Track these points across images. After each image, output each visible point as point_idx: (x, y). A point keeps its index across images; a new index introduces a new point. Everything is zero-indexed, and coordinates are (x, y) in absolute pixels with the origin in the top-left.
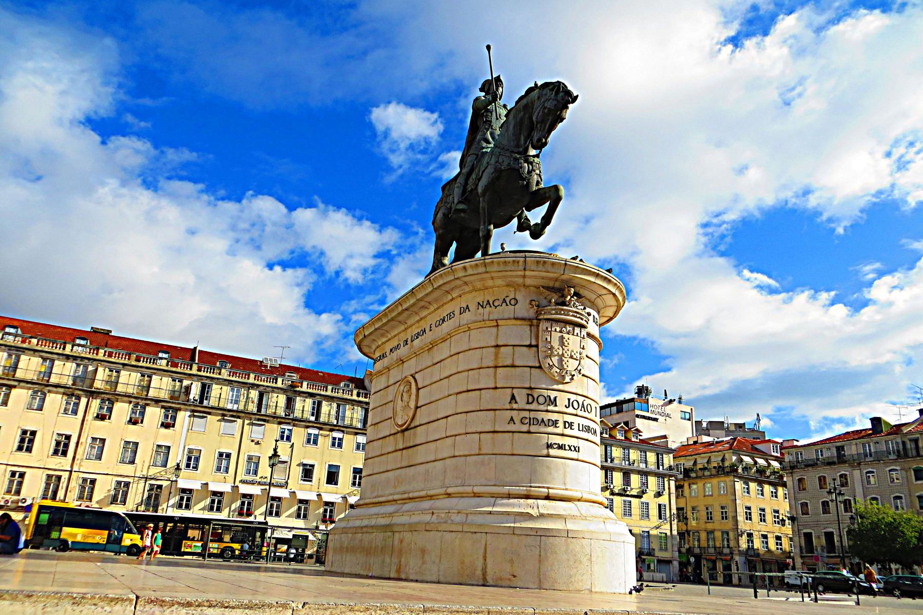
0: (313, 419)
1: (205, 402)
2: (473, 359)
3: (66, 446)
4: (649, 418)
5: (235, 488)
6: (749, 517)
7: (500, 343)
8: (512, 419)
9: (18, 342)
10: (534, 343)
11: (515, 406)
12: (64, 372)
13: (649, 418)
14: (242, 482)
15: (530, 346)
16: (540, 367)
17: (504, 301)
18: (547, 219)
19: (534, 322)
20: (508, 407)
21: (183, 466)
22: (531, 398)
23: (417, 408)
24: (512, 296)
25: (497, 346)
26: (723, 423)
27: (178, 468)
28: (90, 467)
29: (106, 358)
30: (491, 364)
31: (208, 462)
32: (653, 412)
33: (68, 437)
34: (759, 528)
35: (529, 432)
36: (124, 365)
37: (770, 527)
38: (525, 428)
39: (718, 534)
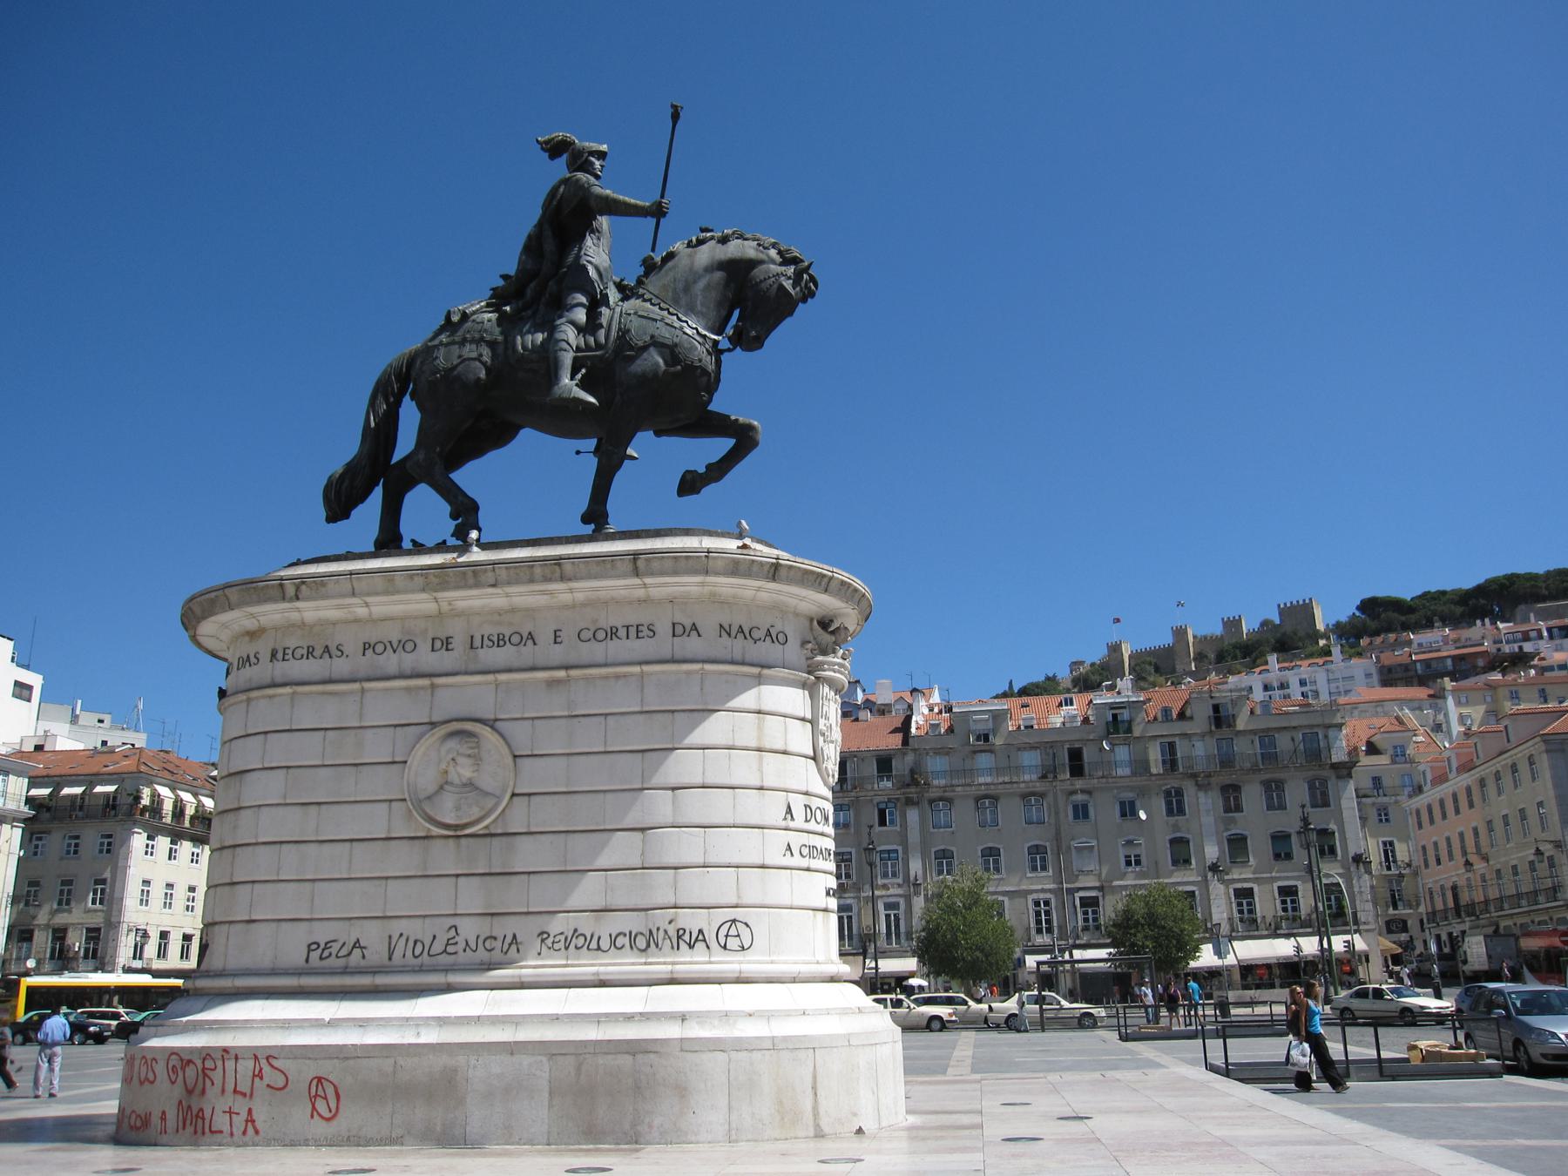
6: (145, 901)
7: (765, 708)
8: (789, 848)
10: (809, 716)
11: (792, 824)
15: (803, 719)
16: (814, 758)
17: (769, 633)
18: (718, 470)
20: (783, 824)
23: (514, 795)
24: (779, 627)
25: (759, 712)
30: (754, 744)
35: (808, 870)
38: (804, 863)
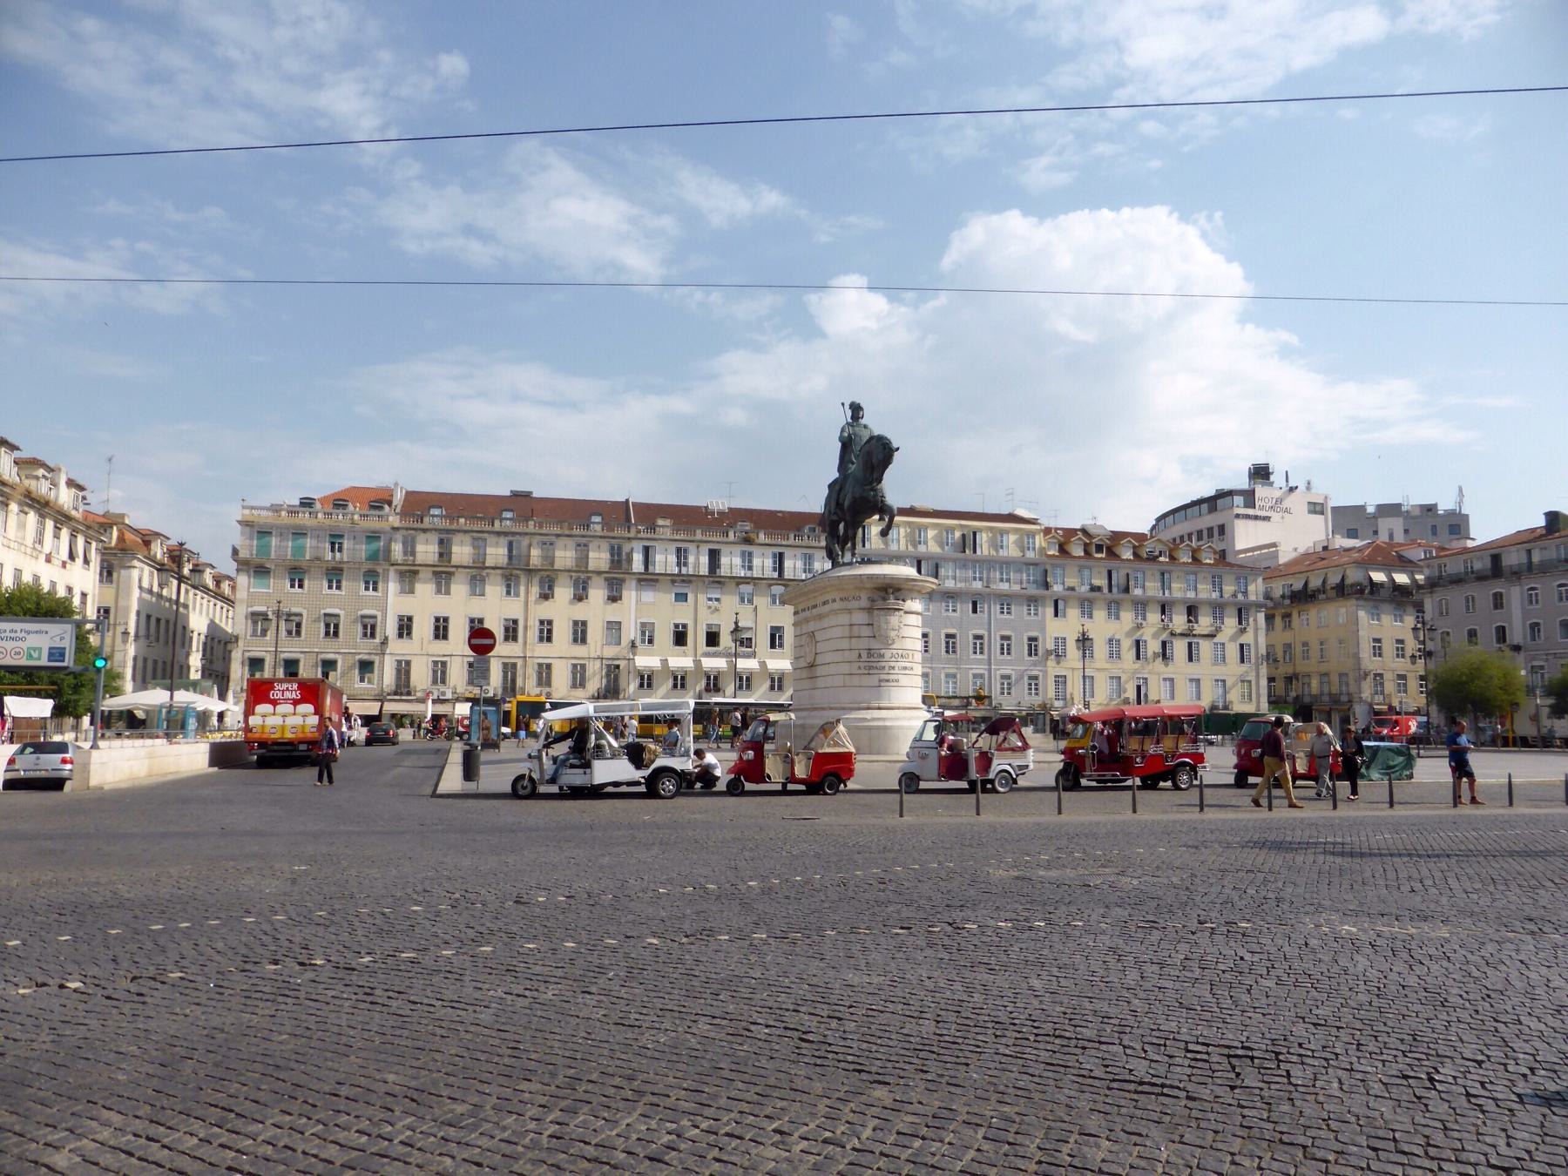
0: (776, 575)
1: (651, 569)
2: (837, 632)
3: (515, 630)
4: (1256, 518)
5: (697, 663)
9: (445, 524)
12: (496, 553)
13: (1256, 518)
14: (707, 655)
19: (870, 610)
21: (638, 643)
22: (870, 655)
26: (1399, 505)
27: (633, 645)
28: (542, 651)
29: (537, 530)
31: (664, 636)
32: (1262, 508)
33: (515, 622)
34: (1393, 666)
36: (558, 536)
37: (1391, 664)
39: (1335, 679)
